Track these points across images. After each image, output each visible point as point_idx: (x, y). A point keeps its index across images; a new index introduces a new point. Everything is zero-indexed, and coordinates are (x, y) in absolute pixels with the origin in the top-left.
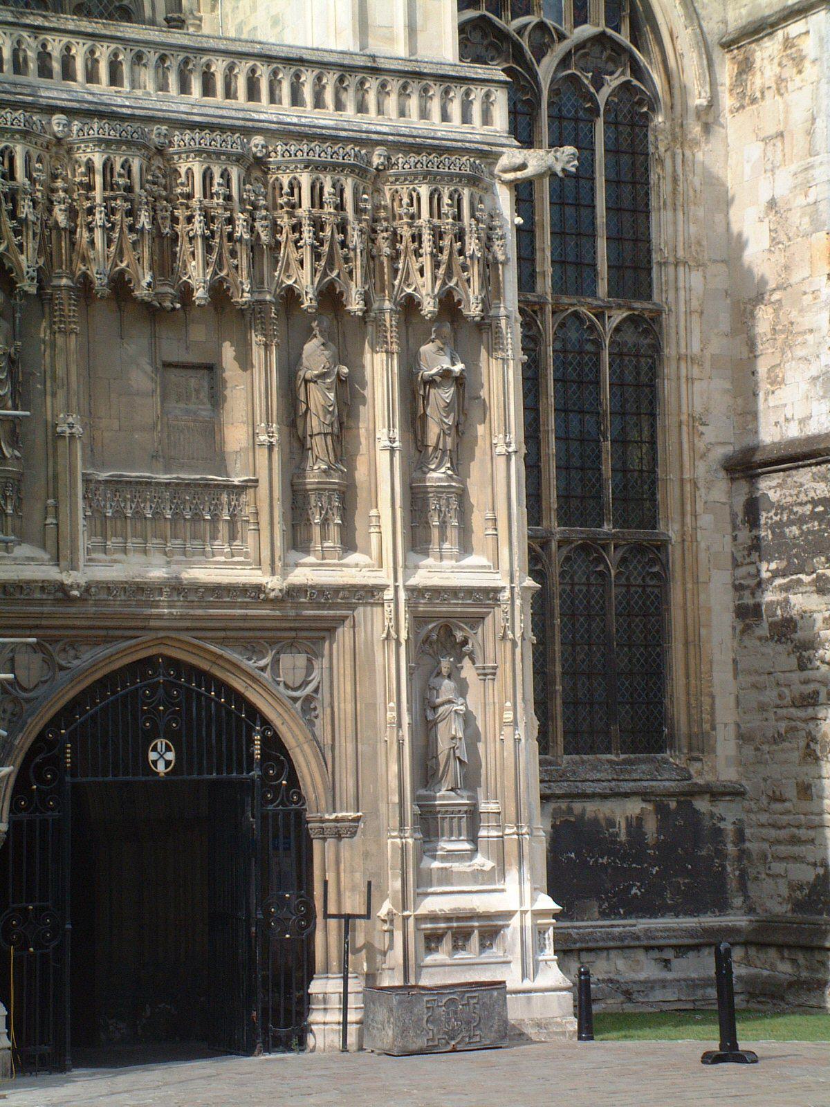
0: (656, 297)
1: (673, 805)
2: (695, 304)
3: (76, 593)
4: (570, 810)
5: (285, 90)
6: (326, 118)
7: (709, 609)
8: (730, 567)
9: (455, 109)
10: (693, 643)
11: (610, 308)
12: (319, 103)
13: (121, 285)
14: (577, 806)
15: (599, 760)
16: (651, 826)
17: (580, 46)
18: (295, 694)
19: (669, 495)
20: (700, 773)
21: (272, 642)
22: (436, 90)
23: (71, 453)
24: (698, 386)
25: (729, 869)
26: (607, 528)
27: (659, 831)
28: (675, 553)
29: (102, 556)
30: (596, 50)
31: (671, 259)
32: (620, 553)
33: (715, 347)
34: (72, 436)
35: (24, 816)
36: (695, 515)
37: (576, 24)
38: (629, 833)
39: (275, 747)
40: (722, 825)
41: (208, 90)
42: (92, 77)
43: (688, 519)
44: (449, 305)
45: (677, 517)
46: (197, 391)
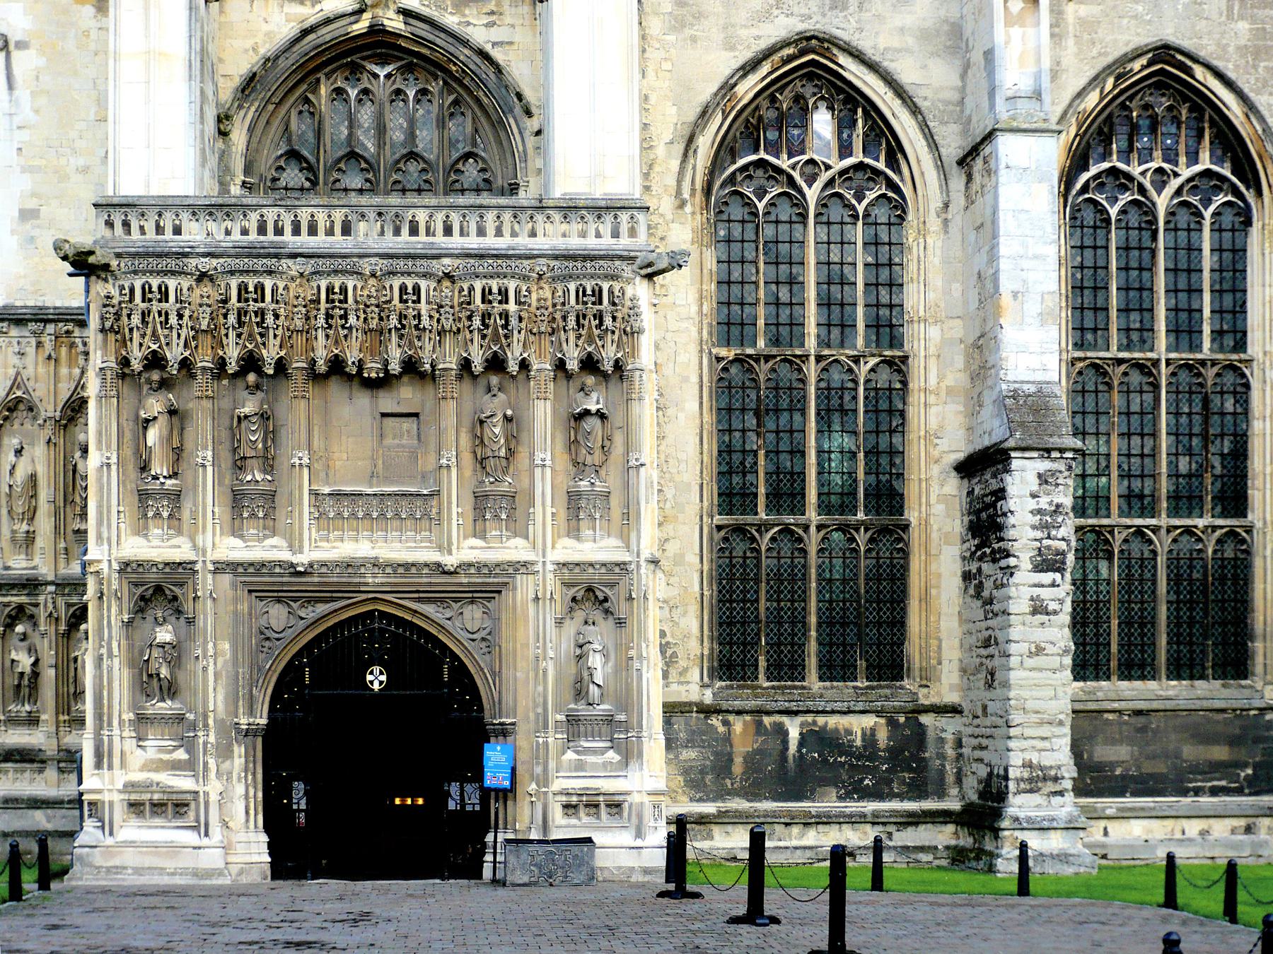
0: (906, 348)
1: (902, 720)
2: (932, 350)
3: (300, 569)
4: (815, 723)
5: (473, 228)
6: (503, 243)
7: (939, 575)
8: (959, 542)
9: (606, 228)
10: (926, 599)
11: (864, 356)
12: (499, 233)
13: (337, 365)
14: (821, 720)
15: (847, 687)
16: (882, 736)
17: (842, 173)
18: (474, 636)
19: (912, 491)
20: (926, 697)
21: (456, 600)
22: (590, 217)
23: (301, 477)
24: (933, 411)
25: (948, 767)
26: (861, 516)
27: (889, 739)
28: (915, 535)
29: (324, 544)
30: (860, 175)
31: (916, 319)
32: (869, 534)
33: (950, 380)
34: (301, 465)
35: (279, 715)
36: (928, 504)
37: (842, 156)
38: (863, 740)
39: (461, 673)
40: (943, 735)
41: (414, 231)
42: (330, 232)
43: (923, 509)
44: (590, 364)
45: (917, 507)
46: (408, 432)
